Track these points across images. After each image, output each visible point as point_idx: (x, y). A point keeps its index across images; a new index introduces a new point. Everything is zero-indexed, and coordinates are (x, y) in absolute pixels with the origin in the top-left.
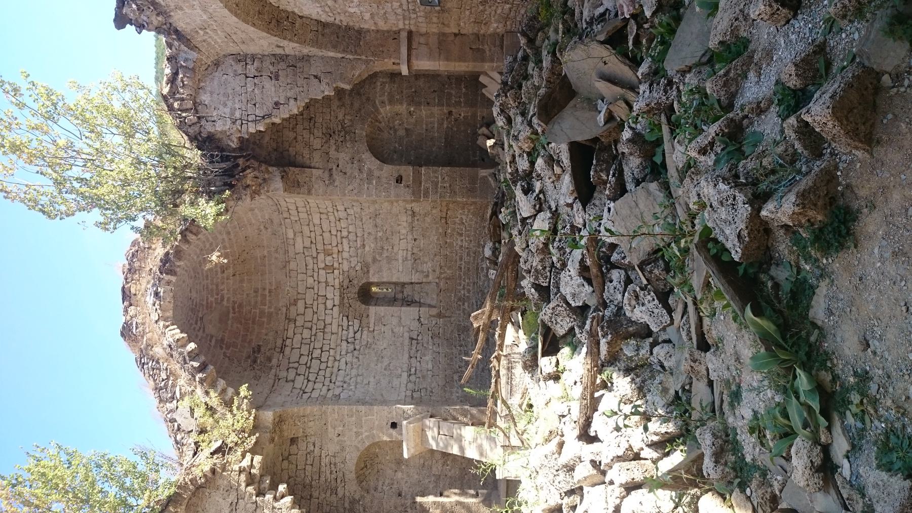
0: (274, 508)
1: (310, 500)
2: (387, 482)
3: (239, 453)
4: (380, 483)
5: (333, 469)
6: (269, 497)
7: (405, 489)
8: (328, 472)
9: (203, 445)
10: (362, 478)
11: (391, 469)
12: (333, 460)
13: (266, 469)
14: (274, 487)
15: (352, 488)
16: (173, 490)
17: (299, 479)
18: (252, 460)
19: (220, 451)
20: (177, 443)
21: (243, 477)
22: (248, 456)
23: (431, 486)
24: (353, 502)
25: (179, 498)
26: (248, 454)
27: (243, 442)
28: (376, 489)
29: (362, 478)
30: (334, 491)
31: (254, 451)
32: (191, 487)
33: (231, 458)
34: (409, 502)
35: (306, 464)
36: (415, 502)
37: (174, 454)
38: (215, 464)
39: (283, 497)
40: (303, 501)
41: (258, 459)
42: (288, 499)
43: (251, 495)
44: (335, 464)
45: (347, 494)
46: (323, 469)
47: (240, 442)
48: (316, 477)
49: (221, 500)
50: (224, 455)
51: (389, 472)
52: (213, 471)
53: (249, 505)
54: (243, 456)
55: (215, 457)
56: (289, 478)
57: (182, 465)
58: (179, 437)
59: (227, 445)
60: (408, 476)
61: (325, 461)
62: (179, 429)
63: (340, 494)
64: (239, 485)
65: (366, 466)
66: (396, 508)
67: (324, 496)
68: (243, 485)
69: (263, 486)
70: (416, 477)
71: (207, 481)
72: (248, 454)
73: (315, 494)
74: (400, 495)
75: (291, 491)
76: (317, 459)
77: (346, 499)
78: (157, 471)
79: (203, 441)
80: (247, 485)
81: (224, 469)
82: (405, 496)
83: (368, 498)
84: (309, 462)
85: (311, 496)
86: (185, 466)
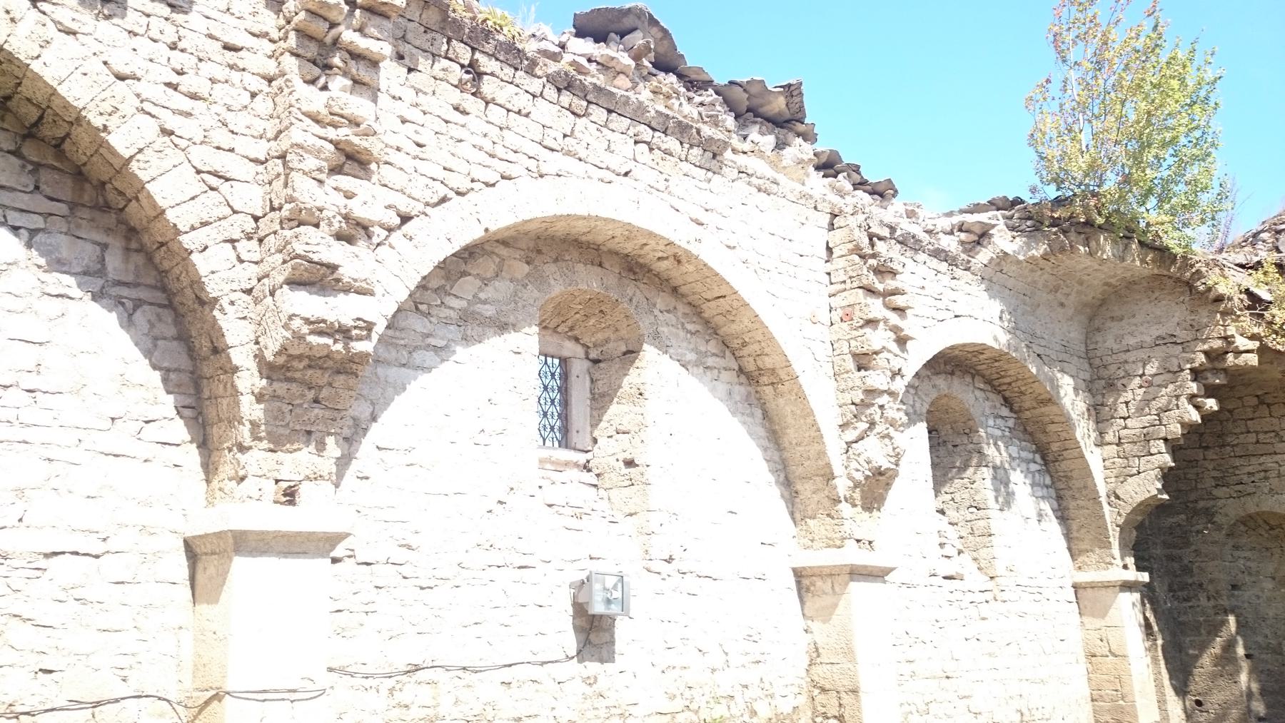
0: (1177, 397)
1: (1201, 447)
2: (1253, 565)
3: (1256, 330)
4: (1248, 554)
5: (1258, 476)
6: (1193, 387)
7: (1247, 594)
8: (1250, 469)
9: (1260, 275)
10: (1252, 524)
11: (1276, 570)
12: (1273, 474)
13: (1239, 377)
14: (1210, 391)
15: (1230, 509)
16: (1178, 251)
17: (1230, 425)
18: (1248, 351)
19: (1255, 301)
20: (1255, 235)
21: (1217, 344)
22: (1255, 345)
23: (1260, 639)
24: (1209, 514)
25: (1168, 262)
26: (1257, 344)
27: (1277, 333)
28: (1236, 547)
29: (1252, 524)
30: (1221, 482)
31: (1263, 351)
32: (1188, 274)
33: (1247, 321)
34: (1225, 602)
35: (1257, 433)
36: (1226, 612)
37: (1236, 234)
38: (1230, 299)
39: (1197, 407)
40: (1195, 437)
41: (1253, 360)
42: (1195, 416)
43: (1192, 361)
44: (1266, 478)
45: (1220, 503)
46: (1254, 460)
47: (1276, 327)
48: (1239, 451)
49: (1176, 320)
50: (1248, 308)
51: (1270, 568)
52: (1219, 299)
53: (1175, 362)
54: (1253, 337)
55: (1244, 296)
56: (1230, 411)
57: (1221, 250)
58: (1264, 236)
59: (1266, 309)
60: (1269, 599)
61: (1269, 462)
62: (1279, 232)
63: (1218, 492)
64: (1204, 341)
65: (1272, 529)
66: (1211, 581)
67: (1211, 467)
68: (1206, 347)
69: (1209, 375)
70: (1271, 614)
71: (1202, 293)
72: (1257, 344)
73: (1211, 454)
74: (1234, 587)
75: (1207, 417)
76: (1270, 449)
77: (1212, 503)
78: (1203, 221)
79: (1265, 273)
80: (1206, 353)
81: (1225, 314)
82: (1233, 595)
83: (1219, 536)
84: (1261, 436)
85: (1207, 448)
86: (1219, 257)
